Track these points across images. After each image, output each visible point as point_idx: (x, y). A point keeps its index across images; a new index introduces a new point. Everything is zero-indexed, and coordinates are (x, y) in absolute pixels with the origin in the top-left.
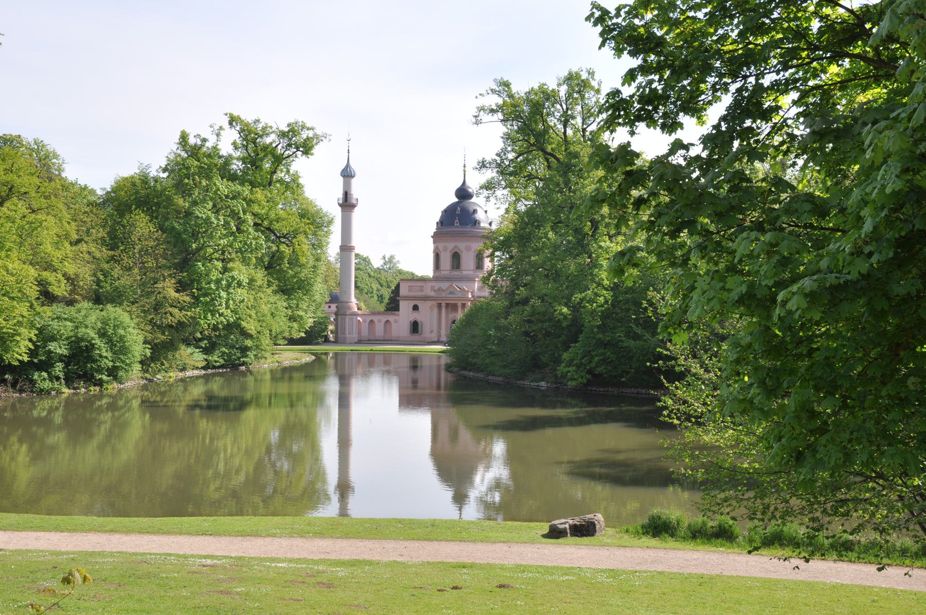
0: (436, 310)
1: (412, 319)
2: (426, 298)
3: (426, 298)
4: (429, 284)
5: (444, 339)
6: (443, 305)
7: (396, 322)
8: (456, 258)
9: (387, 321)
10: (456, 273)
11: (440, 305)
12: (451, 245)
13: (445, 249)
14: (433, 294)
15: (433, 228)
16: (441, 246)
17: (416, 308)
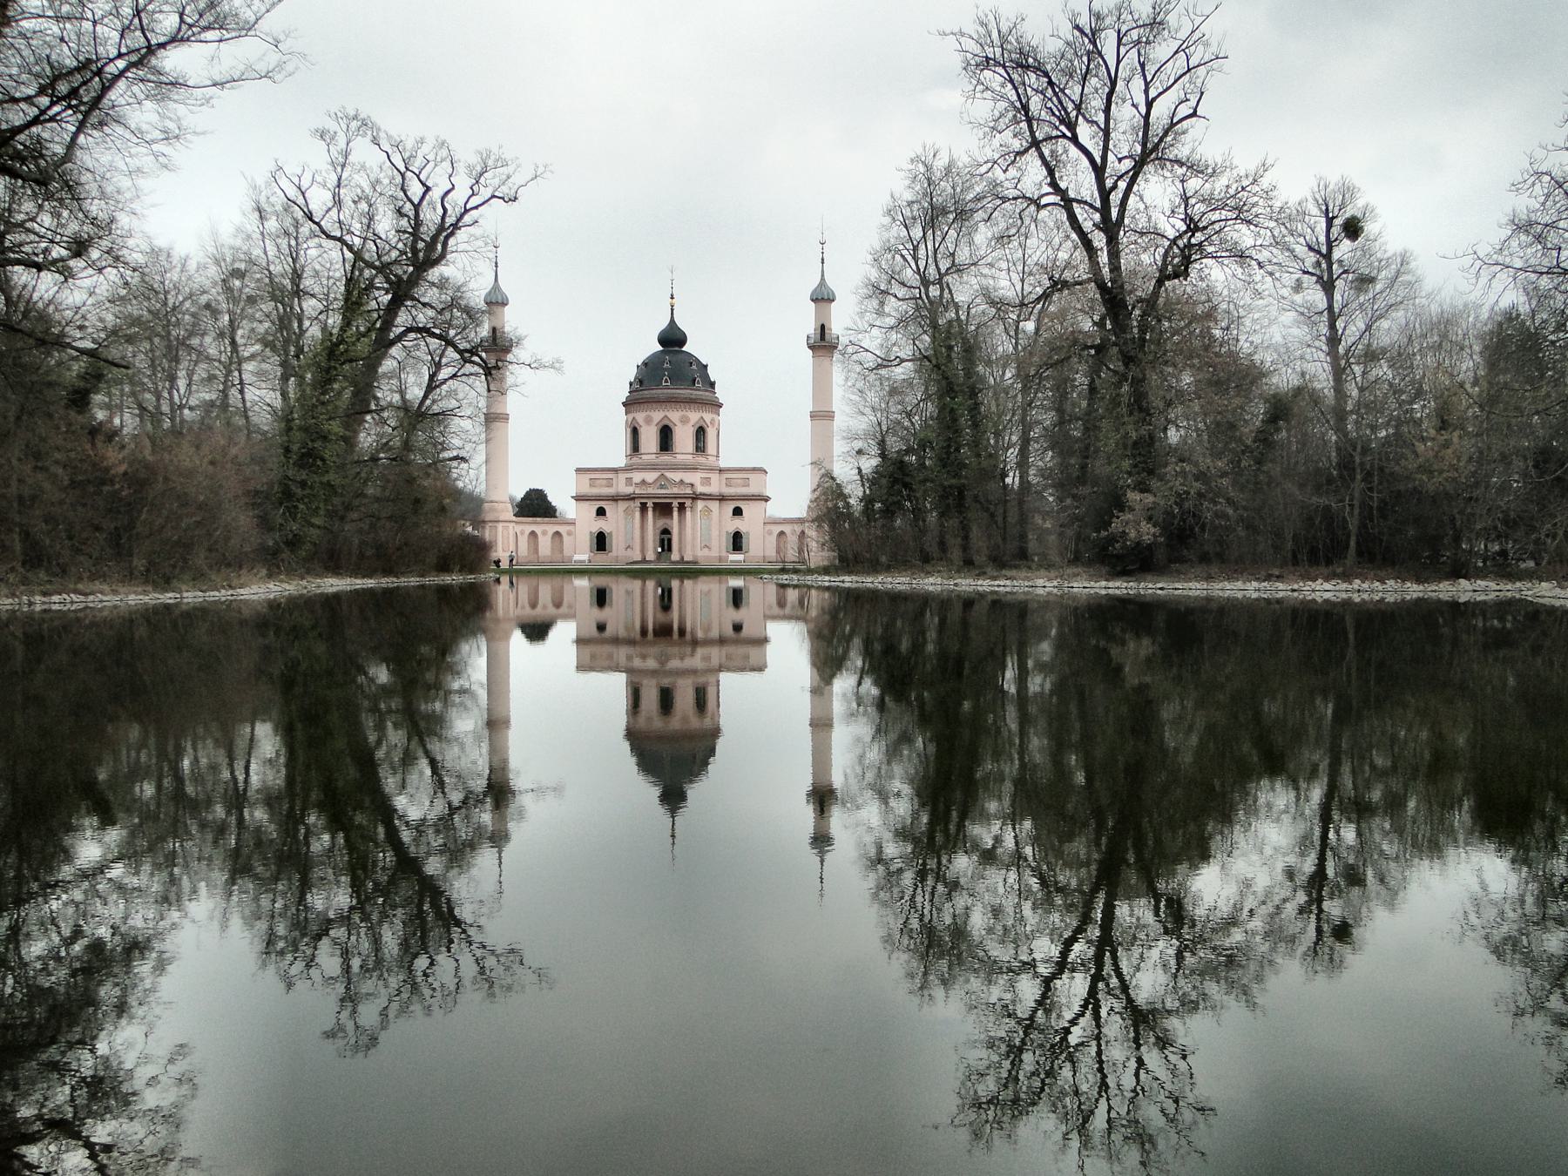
0: (638, 514)
1: (595, 530)
2: (615, 499)
3: (615, 499)
4: (622, 477)
5: (650, 556)
6: (650, 504)
7: (569, 533)
8: (666, 438)
9: (557, 534)
10: (666, 458)
11: (644, 507)
12: (658, 415)
13: (648, 421)
14: (629, 490)
15: (624, 393)
16: (640, 417)
17: (601, 512)
